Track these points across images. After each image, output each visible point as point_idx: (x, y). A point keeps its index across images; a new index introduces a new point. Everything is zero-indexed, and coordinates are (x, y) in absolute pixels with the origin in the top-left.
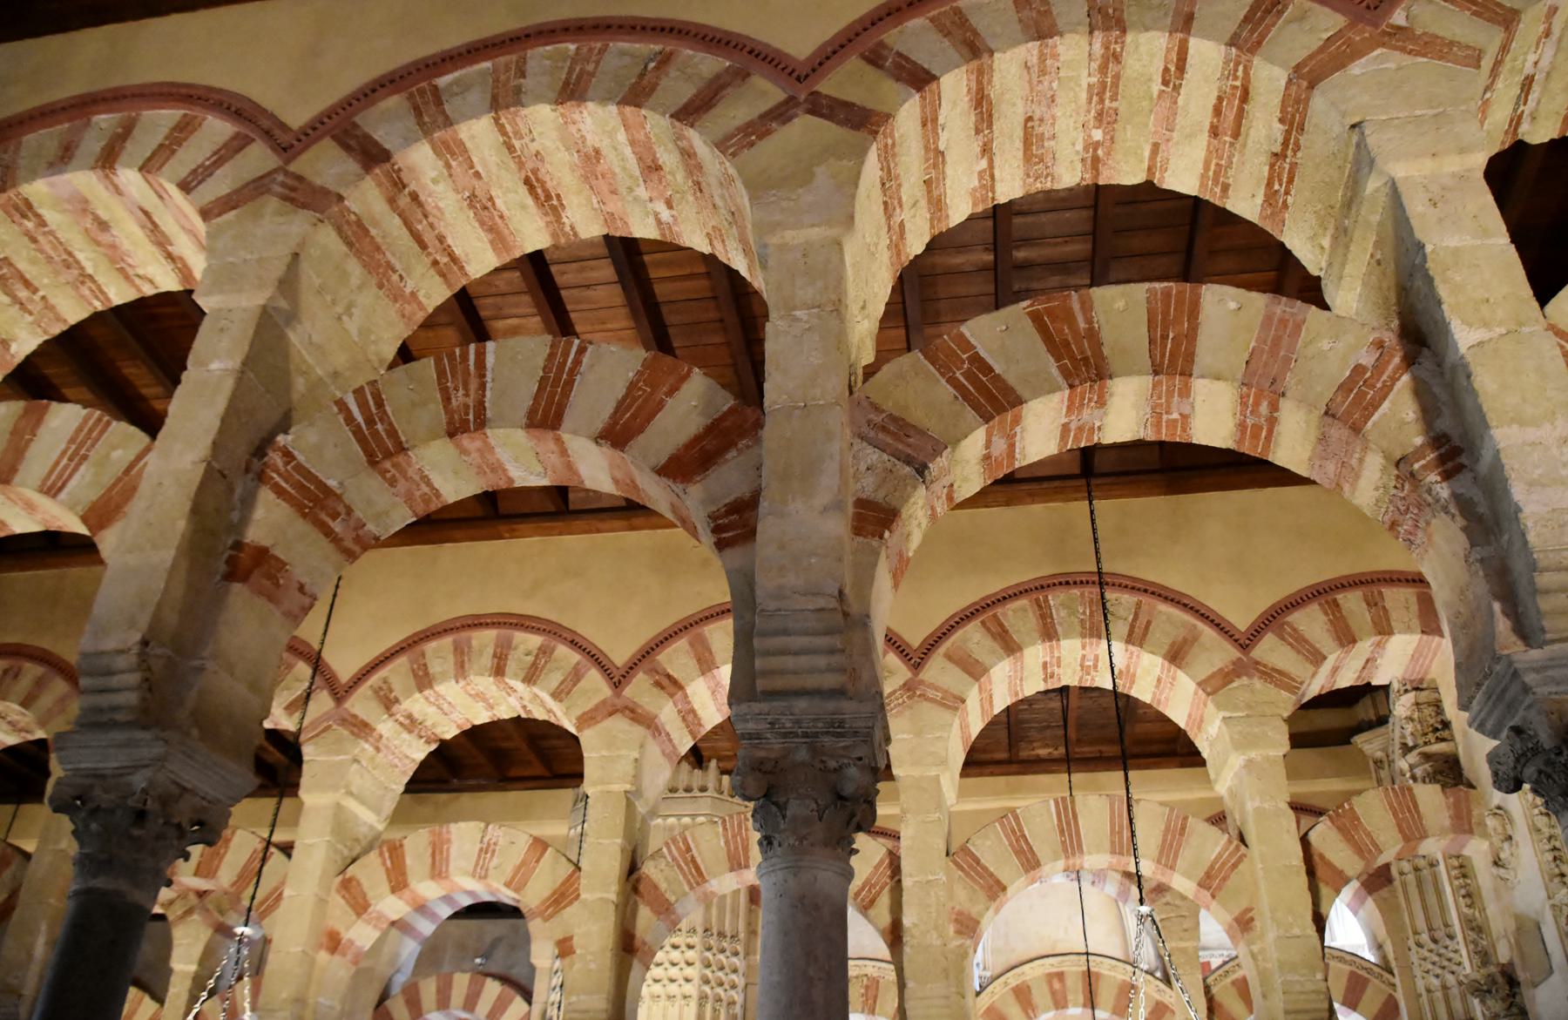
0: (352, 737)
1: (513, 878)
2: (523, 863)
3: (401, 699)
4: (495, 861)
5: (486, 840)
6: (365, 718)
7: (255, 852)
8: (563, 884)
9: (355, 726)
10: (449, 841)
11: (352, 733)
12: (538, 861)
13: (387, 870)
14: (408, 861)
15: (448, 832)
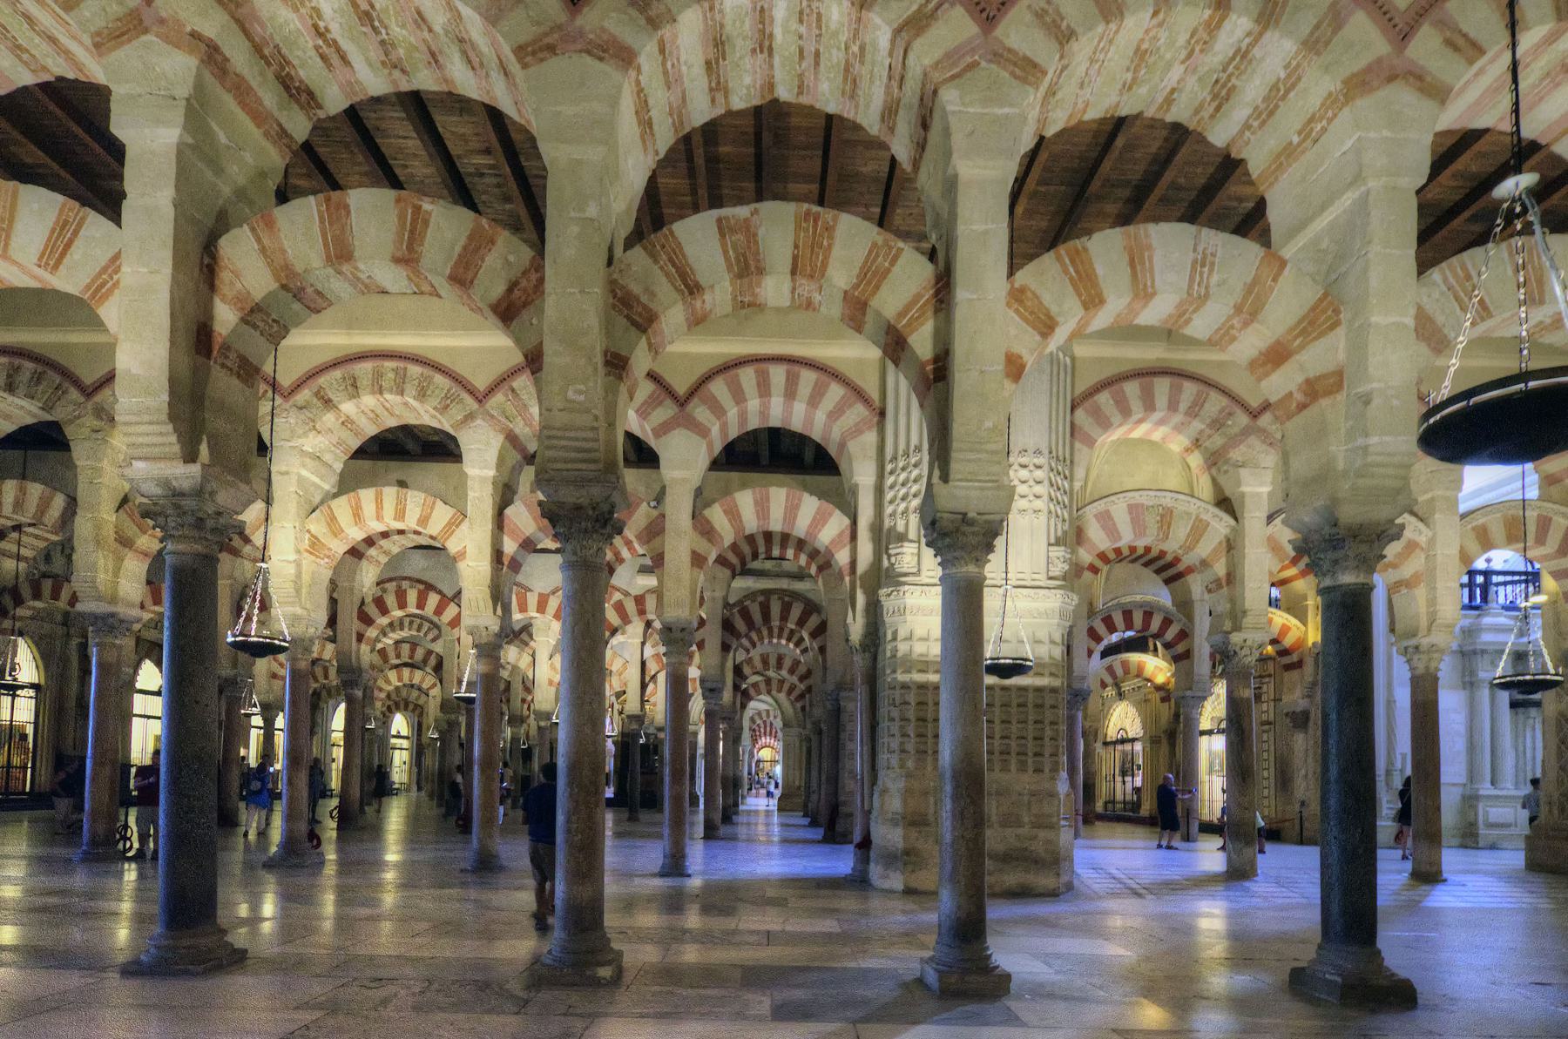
0: (1015, 83)
1: (1245, 298)
2: (1256, 281)
3: (1079, 30)
4: (1215, 278)
5: (1200, 249)
6: (1028, 54)
7: (875, 245)
8: (1313, 309)
9: (1015, 64)
10: (1149, 247)
11: (1013, 74)
12: (1275, 280)
13: (1071, 279)
14: (1100, 270)
15: (1147, 236)
